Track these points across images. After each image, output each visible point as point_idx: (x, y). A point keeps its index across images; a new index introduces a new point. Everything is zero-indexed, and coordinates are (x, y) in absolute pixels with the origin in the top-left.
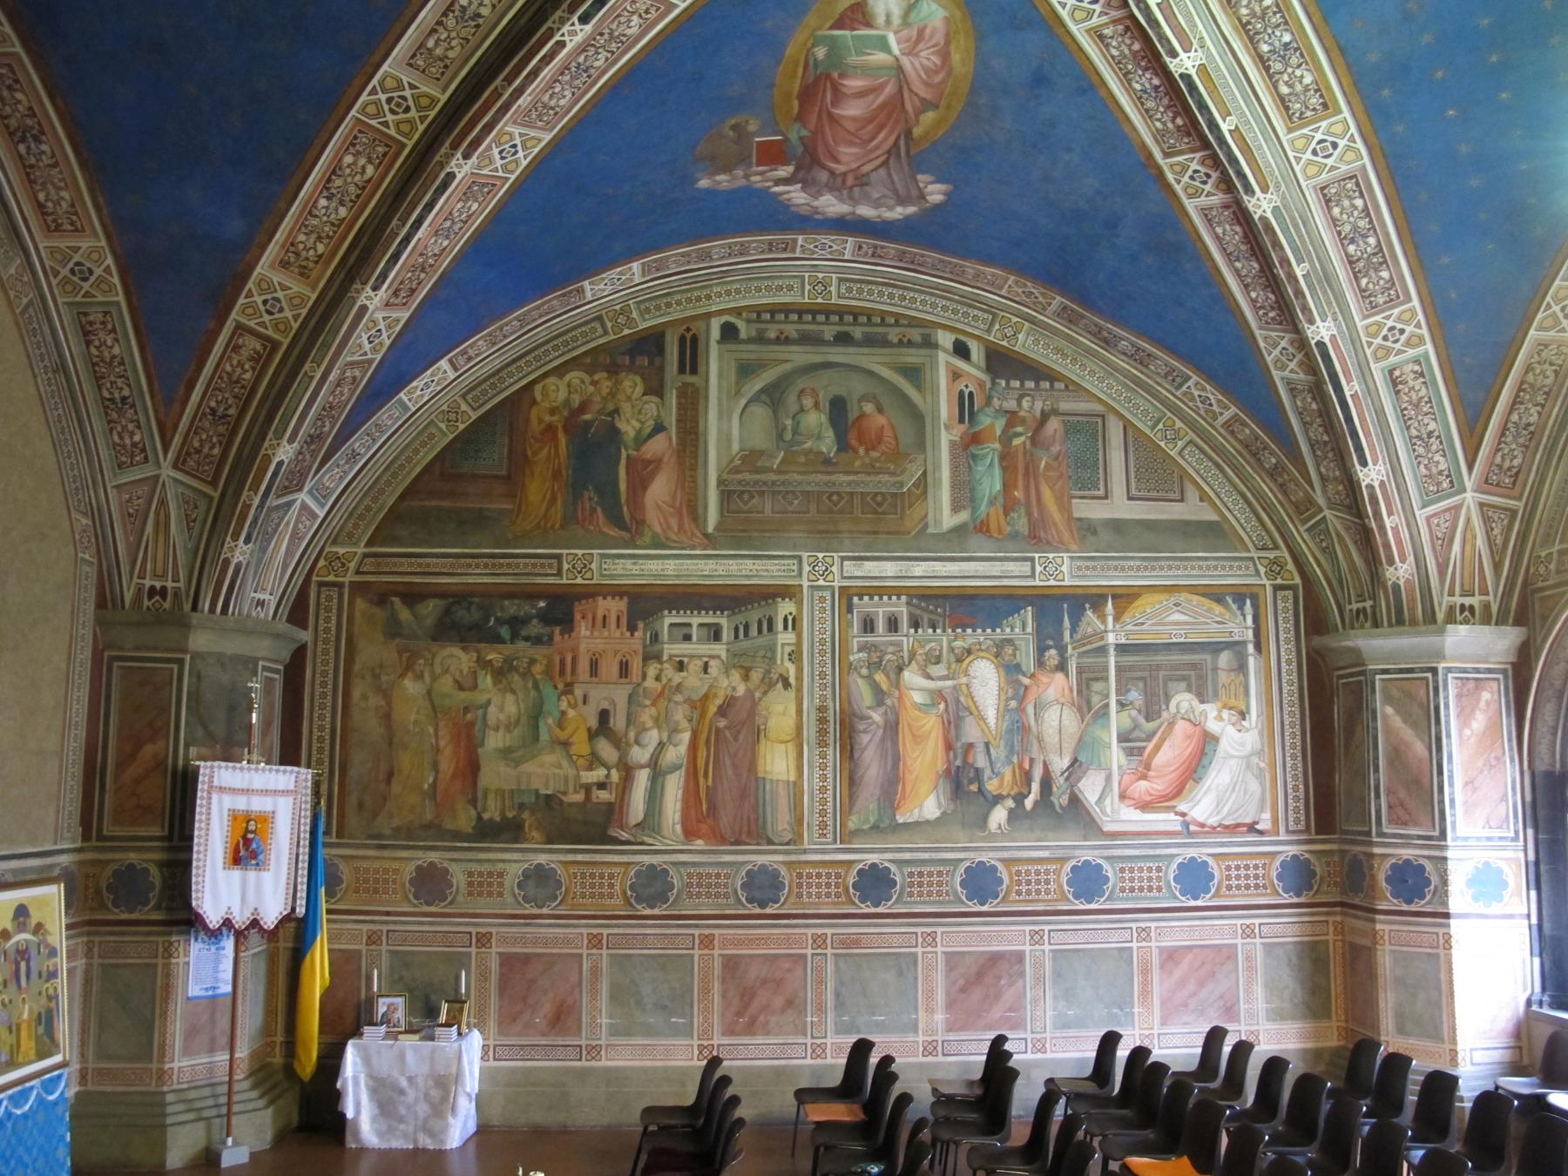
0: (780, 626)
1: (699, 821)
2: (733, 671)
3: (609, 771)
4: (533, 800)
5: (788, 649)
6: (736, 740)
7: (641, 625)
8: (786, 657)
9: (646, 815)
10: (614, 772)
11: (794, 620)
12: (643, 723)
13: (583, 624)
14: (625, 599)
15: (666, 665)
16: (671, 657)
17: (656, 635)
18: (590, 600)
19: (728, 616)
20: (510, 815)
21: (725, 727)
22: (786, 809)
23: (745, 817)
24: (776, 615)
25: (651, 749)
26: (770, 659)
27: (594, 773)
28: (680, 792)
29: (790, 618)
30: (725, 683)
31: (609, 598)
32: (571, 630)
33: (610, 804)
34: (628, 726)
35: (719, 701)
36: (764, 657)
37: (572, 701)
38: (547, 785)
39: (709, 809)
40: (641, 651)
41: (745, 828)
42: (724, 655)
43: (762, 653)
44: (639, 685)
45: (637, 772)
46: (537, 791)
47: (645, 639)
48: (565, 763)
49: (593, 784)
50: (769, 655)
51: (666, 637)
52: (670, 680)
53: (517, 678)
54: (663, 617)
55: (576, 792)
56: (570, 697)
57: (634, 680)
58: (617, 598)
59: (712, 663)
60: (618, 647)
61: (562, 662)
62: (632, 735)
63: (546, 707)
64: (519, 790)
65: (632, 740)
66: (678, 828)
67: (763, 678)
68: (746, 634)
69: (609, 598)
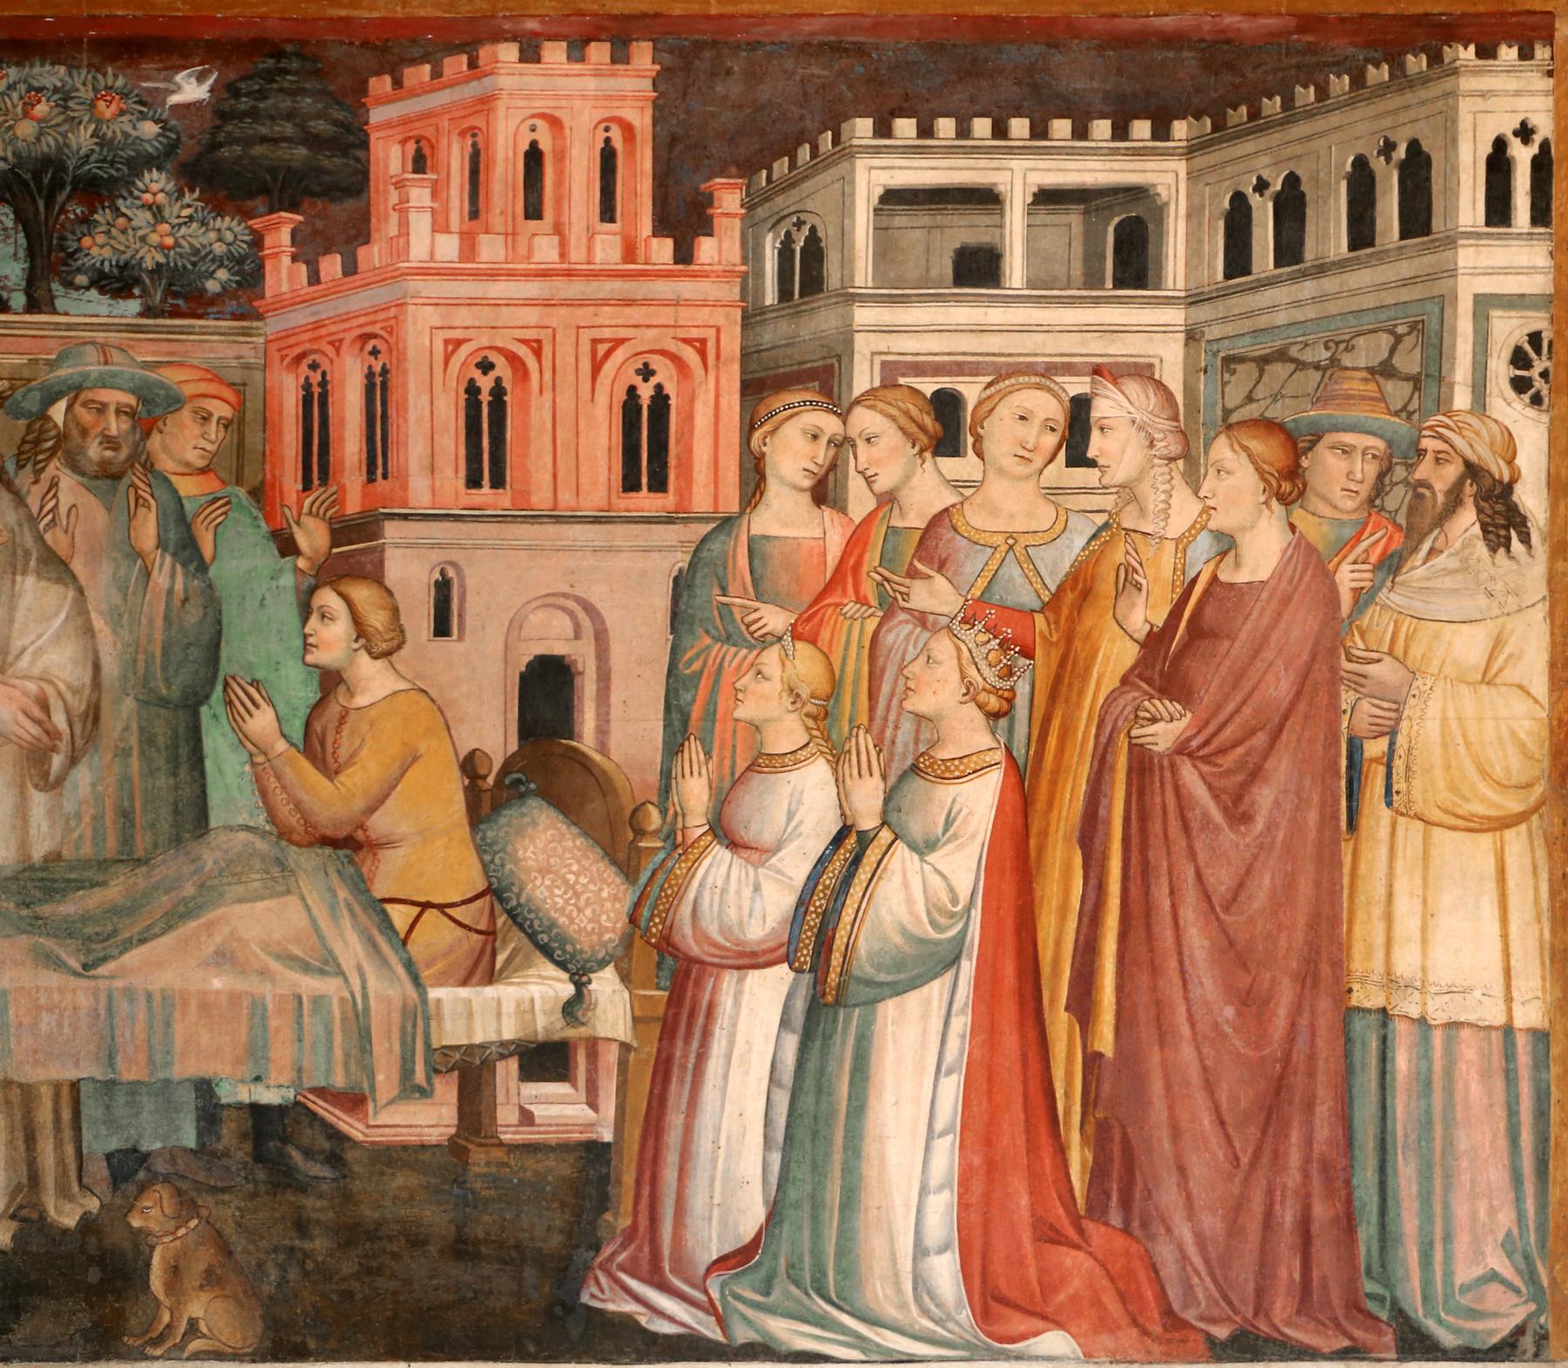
0: (1470, 205)
1: (1049, 1235)
2: (1222, 449)
3: (580, 987)
4: (189, 1137)
5: (1509, 330)
6: (1238, 812)
7: (729, 200)
8: (1500, 369)
9: (774, 1215)
10: (605, 985)
11: (1542, 165)
12: (756, 728)
13: (420, 195)
14: (643, 55)
15: (865, 420)
16: (892, 371)
17: (814, 251)
18: (456, 64)
19: (1192, 150)
20: (67, 1217)
21: (1182, 749)
22: (1496, 1174)
23: (1287, 1217)
24: (1452, 142)
25: (796, 865)
26: (1416, 381)
27: (507, 993)
28: (952, 1088)
29: (1522, 156)
30: (1184, 511)
31: (555, 53)
32: (359, 231)
33: (595, 1152)
34: (674, 747)
35: (1145, 614)
36: (1386, 370)
37: (377, 619)
38: (256, 1054)
39: (1098, 1174)
40: (732, 343)
41: (1288, 1269)
42: (1171, 359)
43: (1371, 350)
44: (727, 523)
45: (729, 980)
46: (204, 1088)
47: (749, 281)
48: (350, 947)
49: (507, 1049)
50: (1409, 362)
51: (863, 274)
52: (888, 500)
53: (70, 489)
54: (845, 152)
55: (412, 1090)
56: (362, 593)
57: (701, 501)
58: (599, 52)
59: (1109, 406)
60: (609, 321)
61: (316, 402)
62: (695, 793)
63: (237, 654)
64: (110, 1085)
65: (697, 823)
66: (945, 1271)
67: (1380, 488)
68: (1289, 250)
69: (555, 53)
